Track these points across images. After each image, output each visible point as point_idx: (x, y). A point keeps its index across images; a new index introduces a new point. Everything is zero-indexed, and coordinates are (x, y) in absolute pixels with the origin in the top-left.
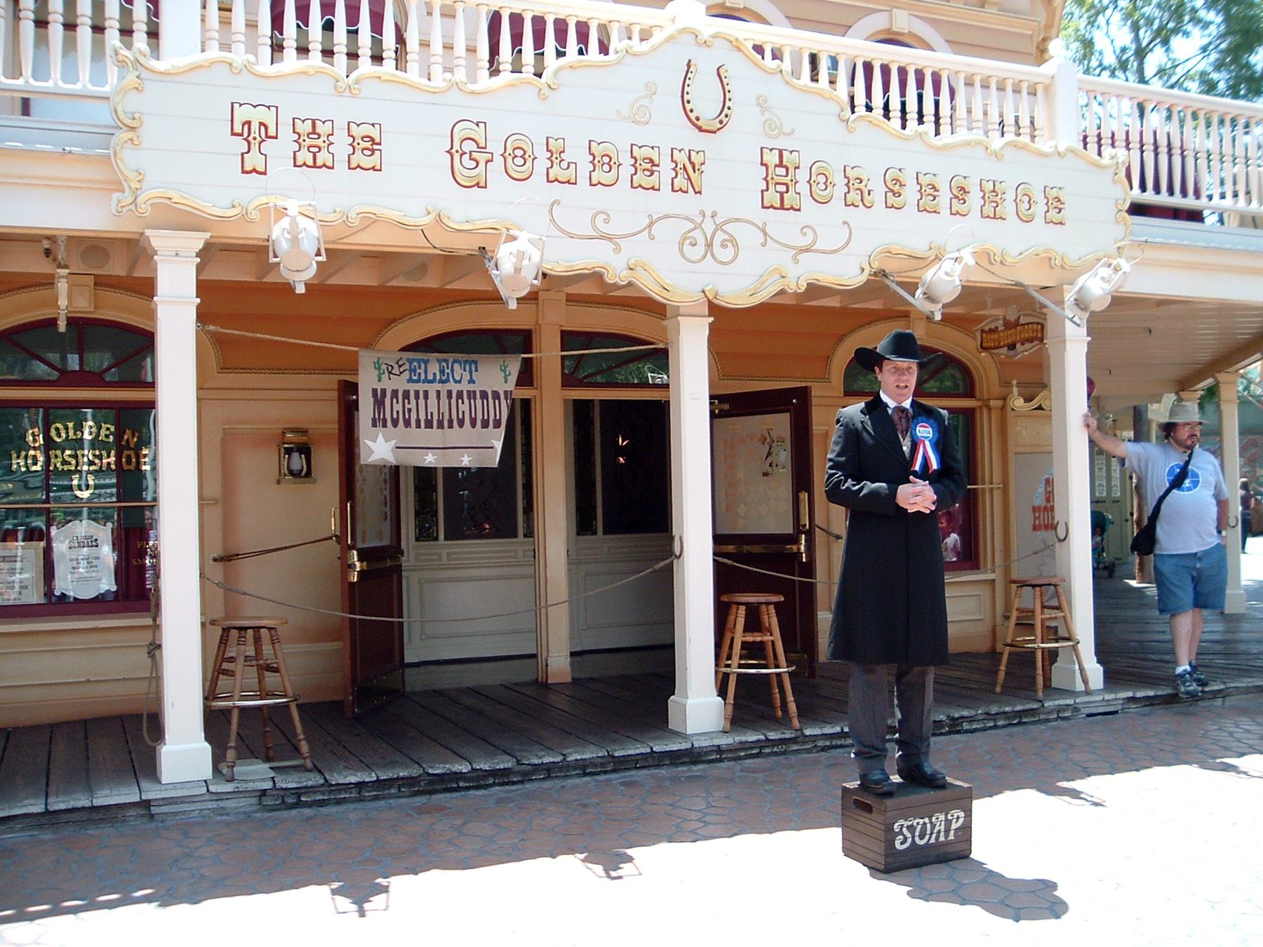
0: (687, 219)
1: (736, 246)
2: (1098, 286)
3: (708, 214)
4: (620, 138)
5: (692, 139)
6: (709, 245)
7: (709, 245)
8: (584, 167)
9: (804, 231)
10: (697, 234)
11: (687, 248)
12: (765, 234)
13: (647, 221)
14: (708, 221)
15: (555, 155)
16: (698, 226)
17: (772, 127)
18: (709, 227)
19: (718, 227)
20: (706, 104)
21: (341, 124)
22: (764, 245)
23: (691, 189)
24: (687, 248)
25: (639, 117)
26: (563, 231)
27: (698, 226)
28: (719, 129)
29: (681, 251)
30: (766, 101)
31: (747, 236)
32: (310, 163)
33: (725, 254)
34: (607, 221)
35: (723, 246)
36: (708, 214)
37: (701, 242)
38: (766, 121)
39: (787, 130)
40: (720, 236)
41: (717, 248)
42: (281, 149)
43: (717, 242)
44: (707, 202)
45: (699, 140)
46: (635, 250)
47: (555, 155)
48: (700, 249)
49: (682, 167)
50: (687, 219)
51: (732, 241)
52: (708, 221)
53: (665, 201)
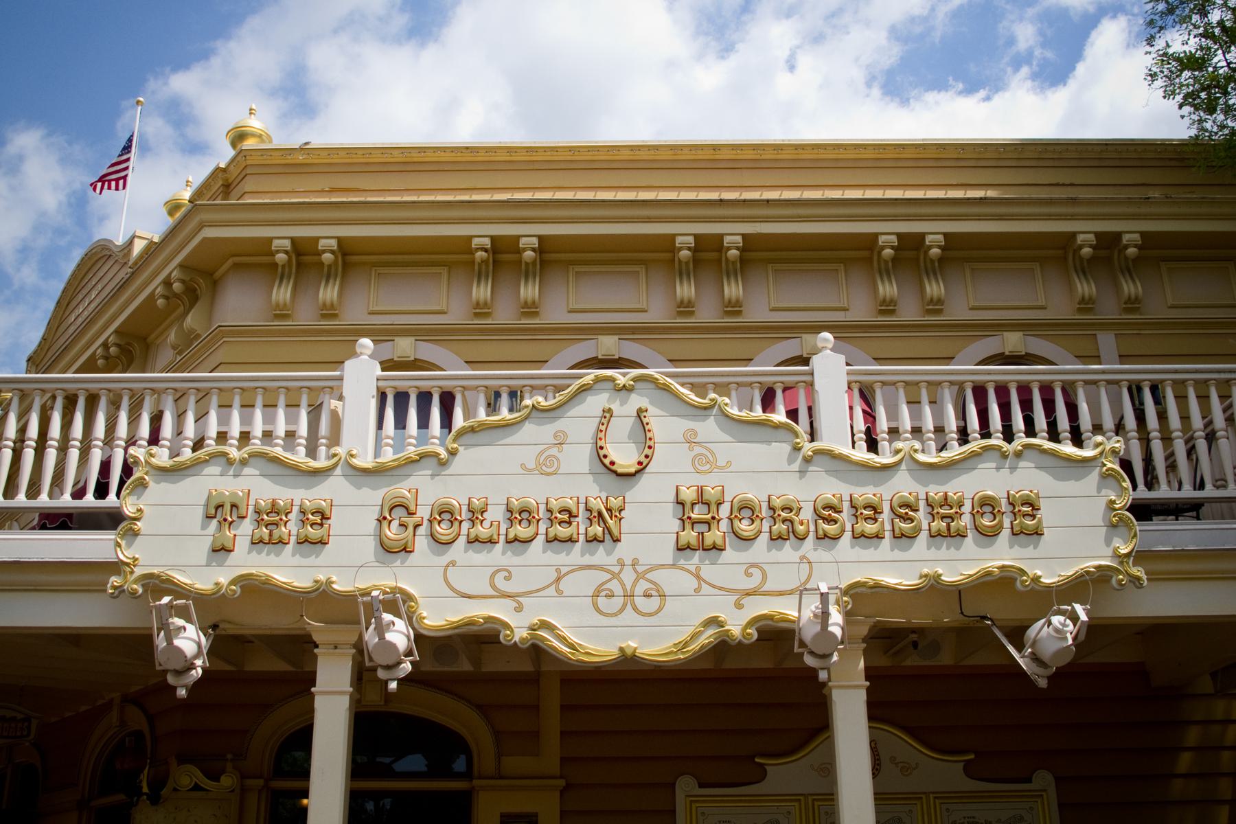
3: (628, 562)
4: (534, 492)
6: (629, 596)
7: (629, 596)
9: (751, 570)
10: (614, 586)
11: (601, 601)
13: (555, 575)
16: (615, 576)
18: (628, 576)
19: (640, 576)
21: (297, 502)
22: (697, 590)
23: (607, 537)
28: (637, 472)
32: (267, 538)
35: (647, 595)
36: (628, 562)
37: (618, 590)
38: (695, 457)
39: (721, 463)
40: (643, 586)
44: (624, 550)
49: (596, 514)
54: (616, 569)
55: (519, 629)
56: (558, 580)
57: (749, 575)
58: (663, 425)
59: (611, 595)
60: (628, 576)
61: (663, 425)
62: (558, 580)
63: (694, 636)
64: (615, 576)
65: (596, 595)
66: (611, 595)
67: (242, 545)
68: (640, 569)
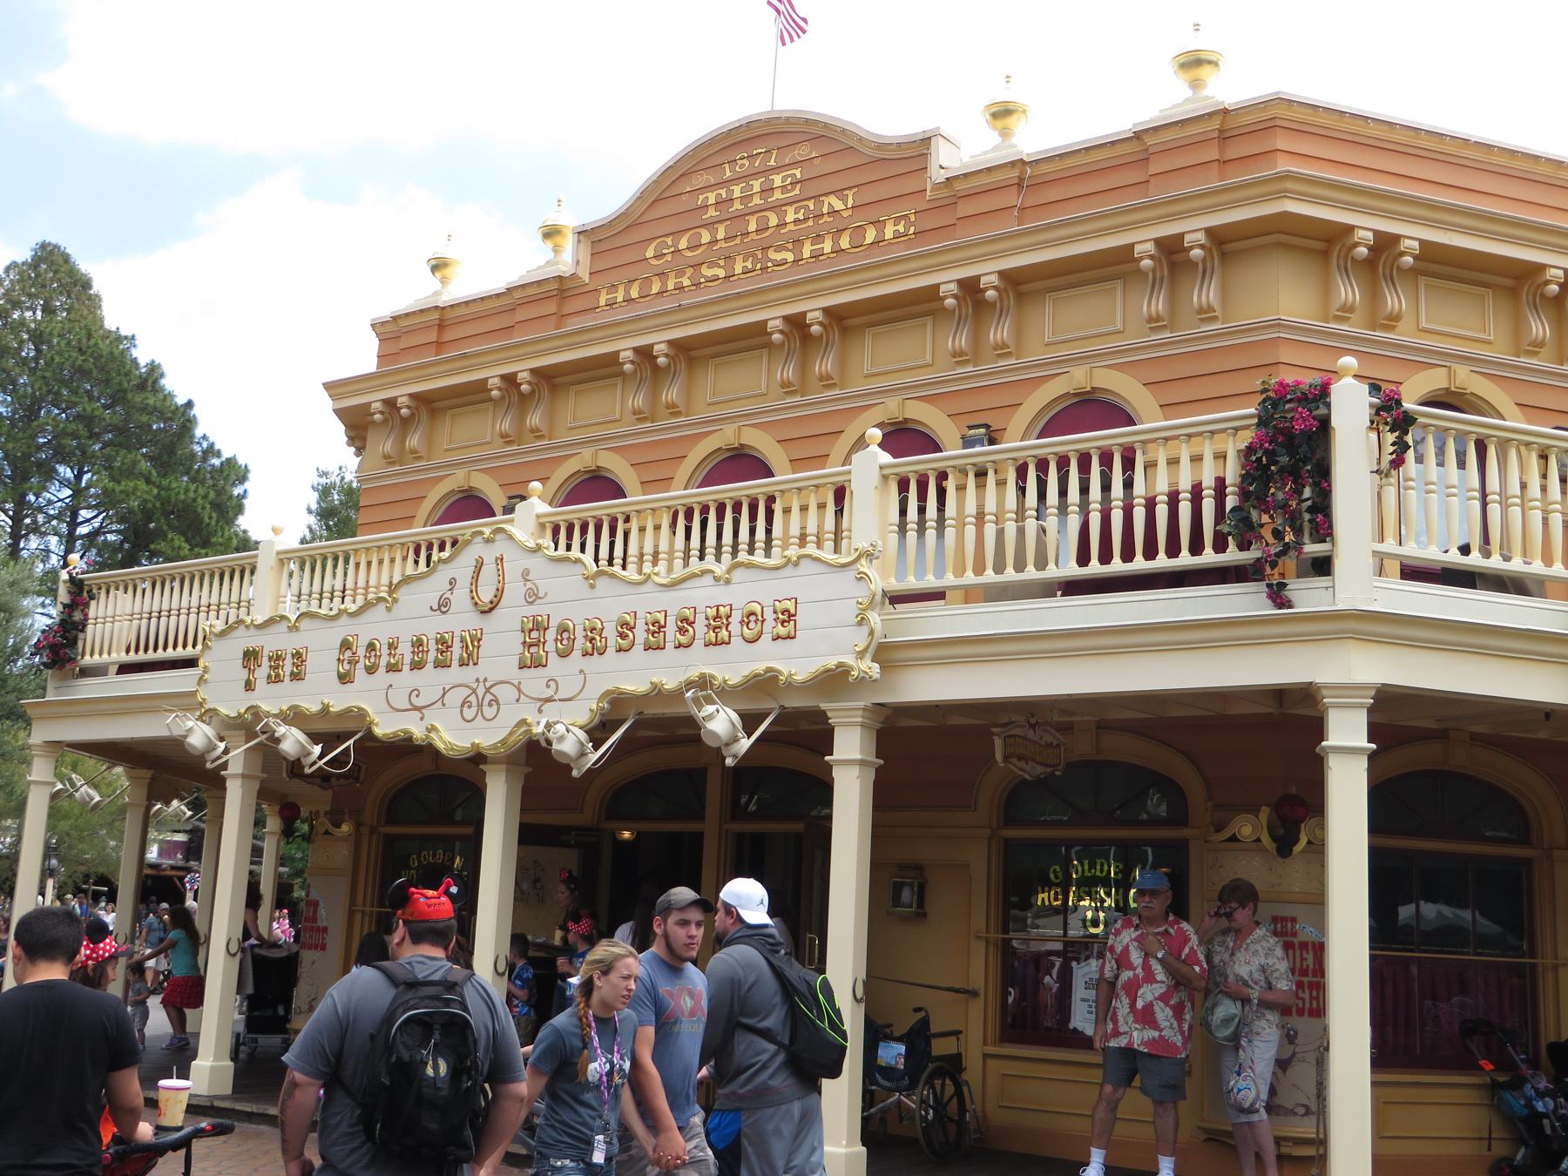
0: (467, 686)
1: (498, 704)
3: (481, 680)
6: (480, 706)
7: (480, 706)
10: (473, 699)
12: (519, 690)
18: (481, 691)
19: (488, 690)
22: (517, 701)
24: (465, 709)
26: (392, 708)
27: (474, 691)
31: (505, 693)
33: (489, 712)
34: (417, 696)
35: (490, 705)
36: (481, 680)
37: (475, 703)
40: (488, 697)
41: (486, 709)
42: (262, 672)
43: (486, 702)
48: (474, 709)
50: (467, 686)
51: (495, 701)
53: (455, 674)
54: (475, 686)
55: (418, 733)
57: (548, 686)
60: (481, 691)
63: (511, 733)
67: (261, 683)
68: (488, 684)
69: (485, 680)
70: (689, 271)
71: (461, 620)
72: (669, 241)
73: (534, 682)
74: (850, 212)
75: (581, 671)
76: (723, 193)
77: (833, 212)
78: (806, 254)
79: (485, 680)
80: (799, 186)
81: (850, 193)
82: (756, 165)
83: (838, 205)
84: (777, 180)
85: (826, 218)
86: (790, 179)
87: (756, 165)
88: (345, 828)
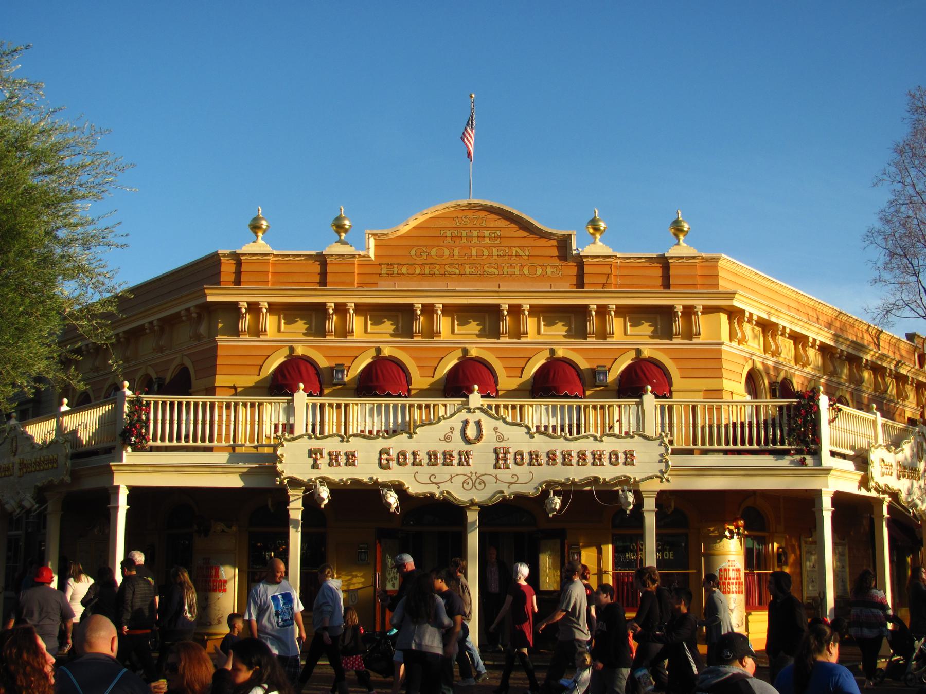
1: (484, 483)
2: (657, 486)
3: (474, 473)
4: (440, 448)
5: (466, 447)
6: (474, 484)
7: (474, 484)
8: (425, 461)
10: (469, 481)
14: (474, 475)
15: (414, 454)
17: (501, 438)
18: (474, 477)
19: (478, 478)
20: (471, 432)
24: (465, 485)
25: (447, 439)
29: (463, 486)
30: (497, 429)
35: (480, 484)
36: (474, 473)
40: (478, 481)
41: (477, 485)
45: (466, 447)
46: (444, 487)
47: (414, 454)
48: (470, 485)
52: (474, 475)
53: (457, 469)
54: (470, 475)
56: (451, 478)
58: (487, 423)
59: (468, 484)
60: (474, 477)
61: (487, 423)
62: (451, 478)
64: (470, 478)
65: (463, 484)
66: (468, 484)
68: (478, 475)
69: (476, 473)
70: (438, 267)
71: (457, 446)
72: (424, 249)
73: (503, 474)
74: (527, 257)
75: (530, 472)
76: (456, 232)
77: (518, 256)
78: (505, 273)
79: (476, 473)
80: (499, 239)
81: (527, 249)
82: (475, 223)
83: (521, 253)
84: (487, 233)
85: (514, 258)
86: (493, 235)
87: (475, 223)
88: (234, 529)
